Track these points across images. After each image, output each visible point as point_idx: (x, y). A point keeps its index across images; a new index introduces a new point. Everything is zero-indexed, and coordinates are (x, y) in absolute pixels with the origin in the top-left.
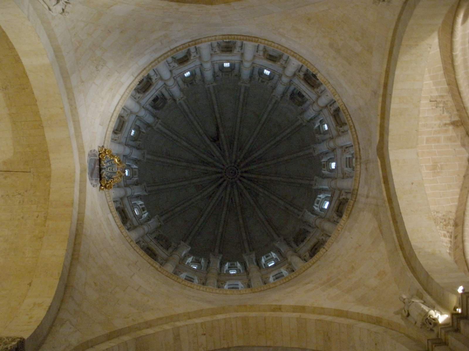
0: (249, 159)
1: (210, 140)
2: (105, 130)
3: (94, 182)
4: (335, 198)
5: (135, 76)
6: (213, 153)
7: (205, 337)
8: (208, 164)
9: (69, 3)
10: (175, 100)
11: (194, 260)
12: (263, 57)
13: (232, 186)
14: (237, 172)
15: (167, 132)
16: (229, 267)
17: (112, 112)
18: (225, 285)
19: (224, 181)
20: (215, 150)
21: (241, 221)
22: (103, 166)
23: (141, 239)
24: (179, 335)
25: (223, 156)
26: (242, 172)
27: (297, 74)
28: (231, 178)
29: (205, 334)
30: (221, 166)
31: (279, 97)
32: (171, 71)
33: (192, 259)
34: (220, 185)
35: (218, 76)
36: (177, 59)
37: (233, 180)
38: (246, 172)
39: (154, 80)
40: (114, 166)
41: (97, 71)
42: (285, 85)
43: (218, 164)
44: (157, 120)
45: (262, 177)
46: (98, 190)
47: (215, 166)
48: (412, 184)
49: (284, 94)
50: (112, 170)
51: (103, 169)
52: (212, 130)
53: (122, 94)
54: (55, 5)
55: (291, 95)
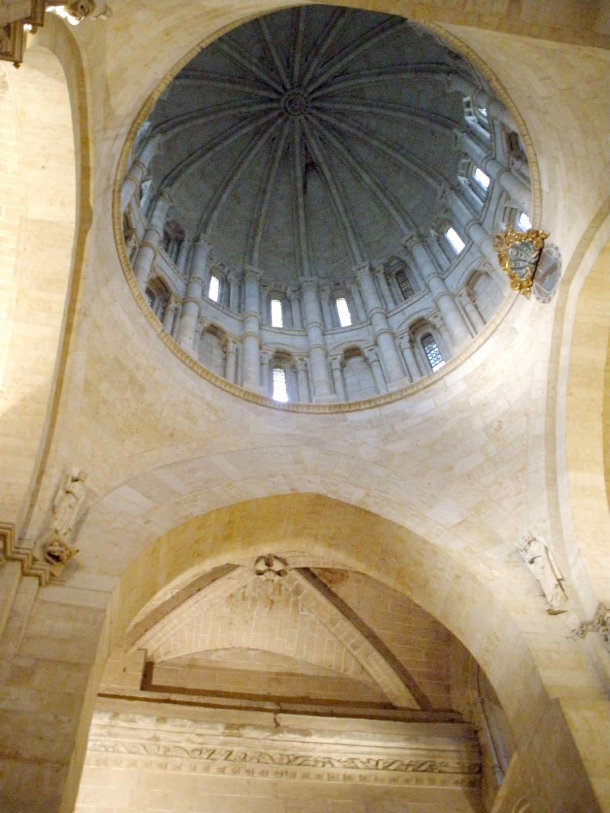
2: (510, 316)
5: (442, 381)
6: (321, 143)
8: (333, 128)
10: (372, 269)
12: (230, 339)
14: (287, 103)
15: (394, 213)
20: (317, 152)
22: (530, 267)
26: (278, 101)
27: (179, 306)
28: (298, 96)
31: (202, 242)
32: (376, 344)
34: (320, 87)
35: (295, 291)
37: (296, 91)
38: (271, 100)
40: (513, 258)
41: (500, 422)
43: (316, 122)
44: (408, 244)
45: (247, 89)
48: (43, 167)
50: (518, 253)
51: (534, 264)
52: (314, 184)
53: (468, 361)
54: (540, 556)
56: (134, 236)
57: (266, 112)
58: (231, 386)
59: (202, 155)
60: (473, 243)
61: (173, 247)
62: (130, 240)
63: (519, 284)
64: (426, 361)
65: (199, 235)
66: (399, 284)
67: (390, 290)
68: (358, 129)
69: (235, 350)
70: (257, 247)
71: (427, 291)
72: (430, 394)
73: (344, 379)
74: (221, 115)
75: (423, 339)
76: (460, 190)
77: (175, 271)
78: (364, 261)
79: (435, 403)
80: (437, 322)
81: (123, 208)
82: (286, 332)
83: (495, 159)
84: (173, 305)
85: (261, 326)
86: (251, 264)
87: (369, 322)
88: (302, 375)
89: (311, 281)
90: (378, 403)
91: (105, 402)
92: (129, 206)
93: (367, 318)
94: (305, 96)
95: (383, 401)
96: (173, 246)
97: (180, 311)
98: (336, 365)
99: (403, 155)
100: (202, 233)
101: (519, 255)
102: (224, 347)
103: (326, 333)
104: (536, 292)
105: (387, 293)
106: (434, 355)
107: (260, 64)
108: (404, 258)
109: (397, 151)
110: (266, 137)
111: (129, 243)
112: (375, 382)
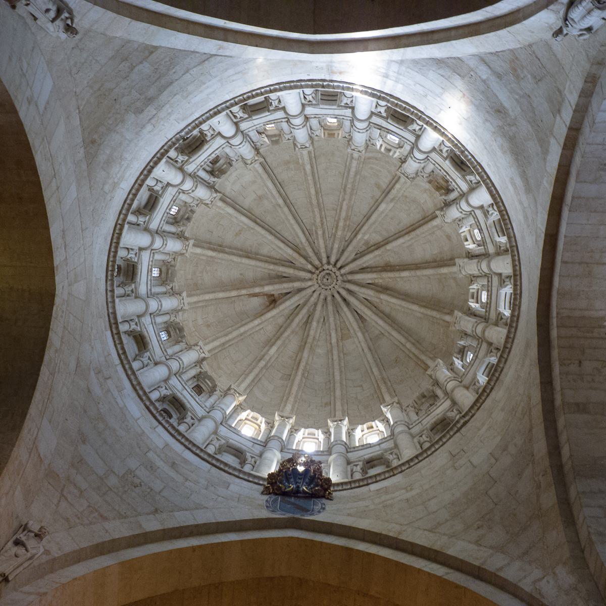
1: (272, 309)
3: (318, 507)
4: (383, 123)
9: (26, 525)
10: (204, 359)
11: (459, 356)
12: (148, 217)
13: (349, 281)
14: (328, 272)
15: (251, 377)
16: (477, 303)
17: (209, 466)
18: (504, 315)
19: (338, 292)
20: (288, 303)
21: (405, 274)
23: (416, 440)
24: (577, 405)
25: (300, 290)
26: (329, 263)
27: (179, 165)
28: (335, 281)
29: (580, 362)
30: (316, 295)
31: (215, 195)
32: (156, 364)
33: (458, 359)
34: (344, 300)
36: (137, 352)
37: (340, 278)
39: (168, 393)
41: (141, 485)
42: (197, 186)
43: (313, 300)
44: (232, 391)
45: (339, 233)
47: (316, 304)
49: (211, 187)
53: (182, 448)
54: (27, 550)
55: (213, 175)
57: (317, 254)
59: (281, 195)
79: (139, 419)
87: (168, 357)
89: (184, 303)
90: (125, 362)
91: (132, 68)
95: (127, 366)
99: (301, 380)
101: (300, 477)
107: (363, 242)
110: (296, 255)
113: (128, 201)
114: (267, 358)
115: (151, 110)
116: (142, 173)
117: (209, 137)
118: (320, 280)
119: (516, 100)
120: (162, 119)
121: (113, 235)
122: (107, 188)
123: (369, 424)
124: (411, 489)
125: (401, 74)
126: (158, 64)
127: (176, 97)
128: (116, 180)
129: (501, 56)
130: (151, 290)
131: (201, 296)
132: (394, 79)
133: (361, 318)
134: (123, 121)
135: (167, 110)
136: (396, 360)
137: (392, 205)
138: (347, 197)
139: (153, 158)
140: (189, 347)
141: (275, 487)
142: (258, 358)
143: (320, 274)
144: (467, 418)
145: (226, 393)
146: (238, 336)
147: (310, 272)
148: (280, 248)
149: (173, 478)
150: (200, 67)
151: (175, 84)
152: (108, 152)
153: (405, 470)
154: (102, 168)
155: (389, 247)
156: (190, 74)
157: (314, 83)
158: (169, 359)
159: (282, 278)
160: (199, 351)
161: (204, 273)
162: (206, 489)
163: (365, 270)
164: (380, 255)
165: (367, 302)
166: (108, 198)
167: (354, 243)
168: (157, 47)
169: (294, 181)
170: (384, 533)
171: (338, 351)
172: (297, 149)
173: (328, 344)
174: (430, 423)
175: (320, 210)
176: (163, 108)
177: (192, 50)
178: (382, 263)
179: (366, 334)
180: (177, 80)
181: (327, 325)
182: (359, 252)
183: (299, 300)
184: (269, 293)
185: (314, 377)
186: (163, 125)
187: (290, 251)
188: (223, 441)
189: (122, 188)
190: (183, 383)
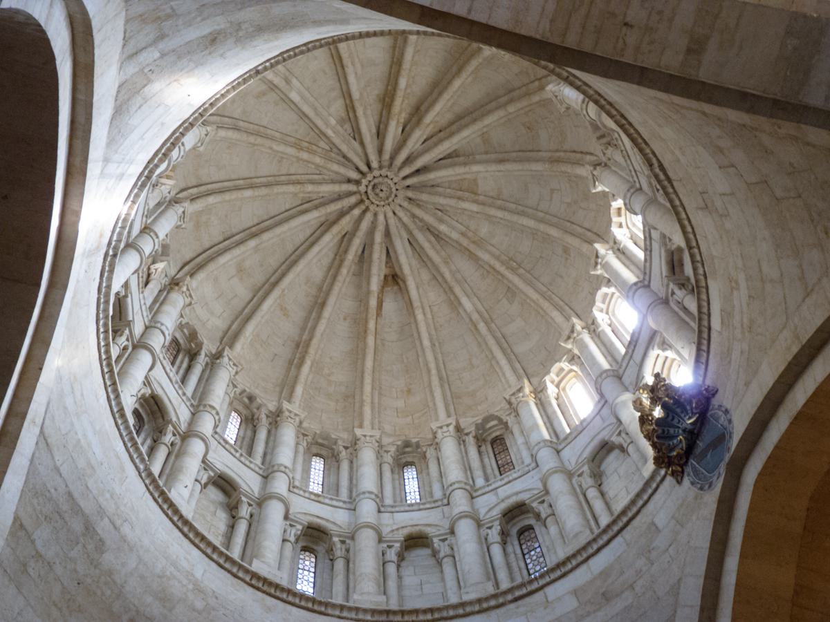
0: (334, 207)
1: (406, 285)
5: (541, 593)
7: (628, 19)
8: (429, 229)
10: (458, 429)
12: (244, 499)
13: (392, 158)
14: (370, 188)
17: (619, 539)
19: (405, 178)
20: (403, 259)
21: (403, 82)
24: (689, 51)
25: (387, 234)
26: (358, 183)
27: (178, 440)
28: (386, 180)
29: (626, 24)
30: (401, 214)
31: (226, 360)
32: (452, 532)
37: (384, 172)
38: (349, 181)
44: (513, 400)
45: (318, 160)
46: (721, 392)
47: (414, 216)
53: (584, 567)
56: (127, 332)
57: (340, 197)
58: (233, 562)
60: (606, 401)
61: (182, 362)
62: (121, 335)
63: (666, 460)
64: (522, 565)
65: (223, 349)
66: (495, 455)
67: (482, 461)
68: (463, 234)
69: (248, 517)
70: (302, 378)
71: (534, 465)
72: (522, 610)
73: (400, 577)
74: (277, 189)
75: (521, 533)
76: (594, 330)
77: (180, 392)
78: (449, 416)
80: (544, 510)
81: (116, 286)
82: (327, 501)
83: (648, 286)
84: (168, 438)
85: (292, 487)
86: (289, 401)
87: (445, 501)
88: (340, 565)
91: (38, 556)
92: (126, 285)
93: (445, 495)
94: (396, 180)
95: (451, 613)
96: (183, 361)
97: (177, 447)
98: (392, 555)
99: (519, 276)
100: (227, 348)
101: (670, 418)
102: (232, 509)
103: (382, 509)
104: (692, 474)
105: (475, 463)
106: (534, 558)
107: (339, 128)
108: (505, 418)
109: (513, 270)
110: (335, 229)
111: (117, 338)
112: (445, 586)
113: (221, 561)
114: (475, 316)
115: (103, 527)
116: (186, 536)
117: (146, 391)
118: (380, 201)
119: (203, 20)
120: (118, 508)
121: (264, 592)
122: (199, 605)
123: (613, 211)
124: (737, 282)
125: (123, 159)
126: (40, 516)
127: (89, 485)
128: (191, 587)
129: (132, 34)
130: (344, 502)
131: (365, 398)
132: (127, 165)
133: (451, 158)
134: (110, 573)
135: (107, 500)
136: (529, 128)
137: (294, 81)
138: (268, 143)
139: (167, 515)
140: (437, 446)
141: (676, 461)
142: (473, 329)
143: (371, 199)
144: (654, 161)
145: (514, 409)
146: (434, 351)
147: (364, 212)
148: (321, 250)
149: (626, 607)
150: (55, 449)
151: (72, 488)
152: (149, 599)
153: (705, 271)
154: (170, 610)
155: (356, 95)
156: (61, 465)
157: (107, 268)
158: (448, 501)
159: (364, 257)
160: (445, 434)
161: (333, 378)
162: (652, 564)
163: (381, 131)
164: (365, 108)
165: (430, 141)
166: (212, 601)
167: (337, 141)
168: (15, 518)
169: (226, 216)
170: (790, 358)
171: (490, 206)
172: (183, 226)
173: (478, 215)
174: (642, 165)
175: (278, 184)
176: (103, 507)
177: (29, 463)
178: (378, 106)
179: (478, 157)
180: (67, 486)
181: (448, 209)
182: (352, 135)
183: (401, 238)
184: (382, 283)
185: (520, 253)
186: (125, 505)
187: (327, 238)
188: (586, 468)
189: (203, 575)
190: (487, 489)
